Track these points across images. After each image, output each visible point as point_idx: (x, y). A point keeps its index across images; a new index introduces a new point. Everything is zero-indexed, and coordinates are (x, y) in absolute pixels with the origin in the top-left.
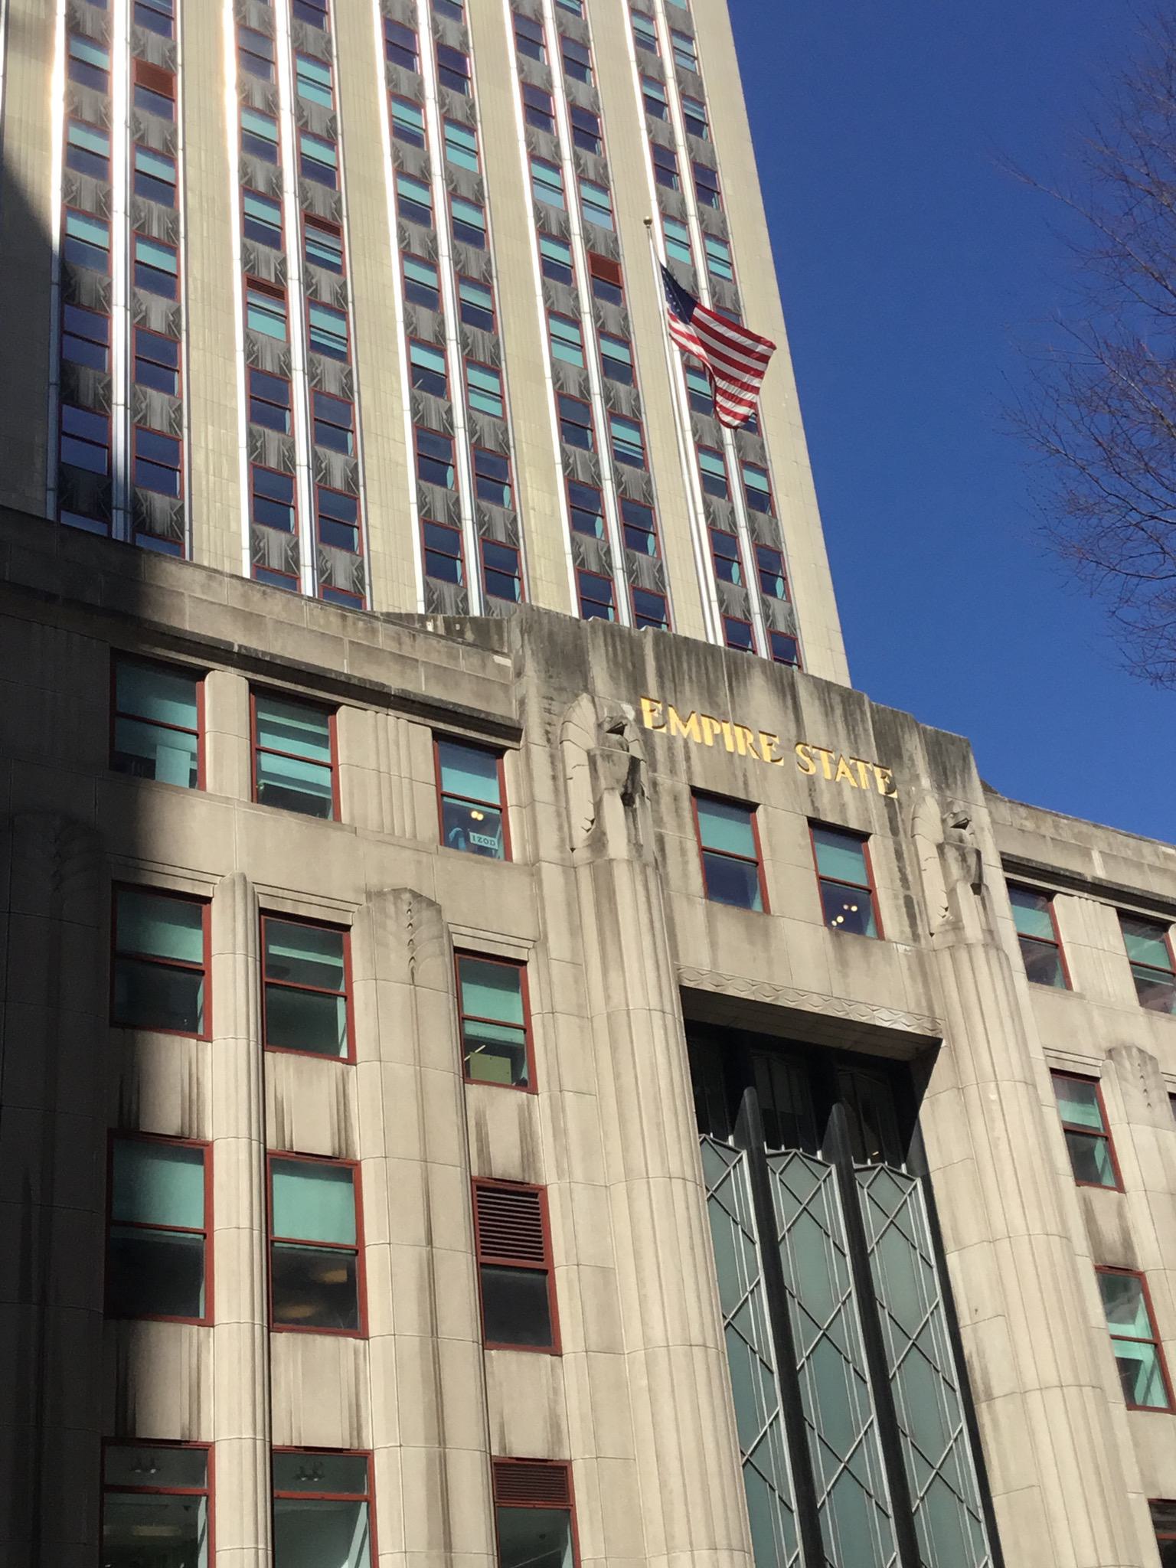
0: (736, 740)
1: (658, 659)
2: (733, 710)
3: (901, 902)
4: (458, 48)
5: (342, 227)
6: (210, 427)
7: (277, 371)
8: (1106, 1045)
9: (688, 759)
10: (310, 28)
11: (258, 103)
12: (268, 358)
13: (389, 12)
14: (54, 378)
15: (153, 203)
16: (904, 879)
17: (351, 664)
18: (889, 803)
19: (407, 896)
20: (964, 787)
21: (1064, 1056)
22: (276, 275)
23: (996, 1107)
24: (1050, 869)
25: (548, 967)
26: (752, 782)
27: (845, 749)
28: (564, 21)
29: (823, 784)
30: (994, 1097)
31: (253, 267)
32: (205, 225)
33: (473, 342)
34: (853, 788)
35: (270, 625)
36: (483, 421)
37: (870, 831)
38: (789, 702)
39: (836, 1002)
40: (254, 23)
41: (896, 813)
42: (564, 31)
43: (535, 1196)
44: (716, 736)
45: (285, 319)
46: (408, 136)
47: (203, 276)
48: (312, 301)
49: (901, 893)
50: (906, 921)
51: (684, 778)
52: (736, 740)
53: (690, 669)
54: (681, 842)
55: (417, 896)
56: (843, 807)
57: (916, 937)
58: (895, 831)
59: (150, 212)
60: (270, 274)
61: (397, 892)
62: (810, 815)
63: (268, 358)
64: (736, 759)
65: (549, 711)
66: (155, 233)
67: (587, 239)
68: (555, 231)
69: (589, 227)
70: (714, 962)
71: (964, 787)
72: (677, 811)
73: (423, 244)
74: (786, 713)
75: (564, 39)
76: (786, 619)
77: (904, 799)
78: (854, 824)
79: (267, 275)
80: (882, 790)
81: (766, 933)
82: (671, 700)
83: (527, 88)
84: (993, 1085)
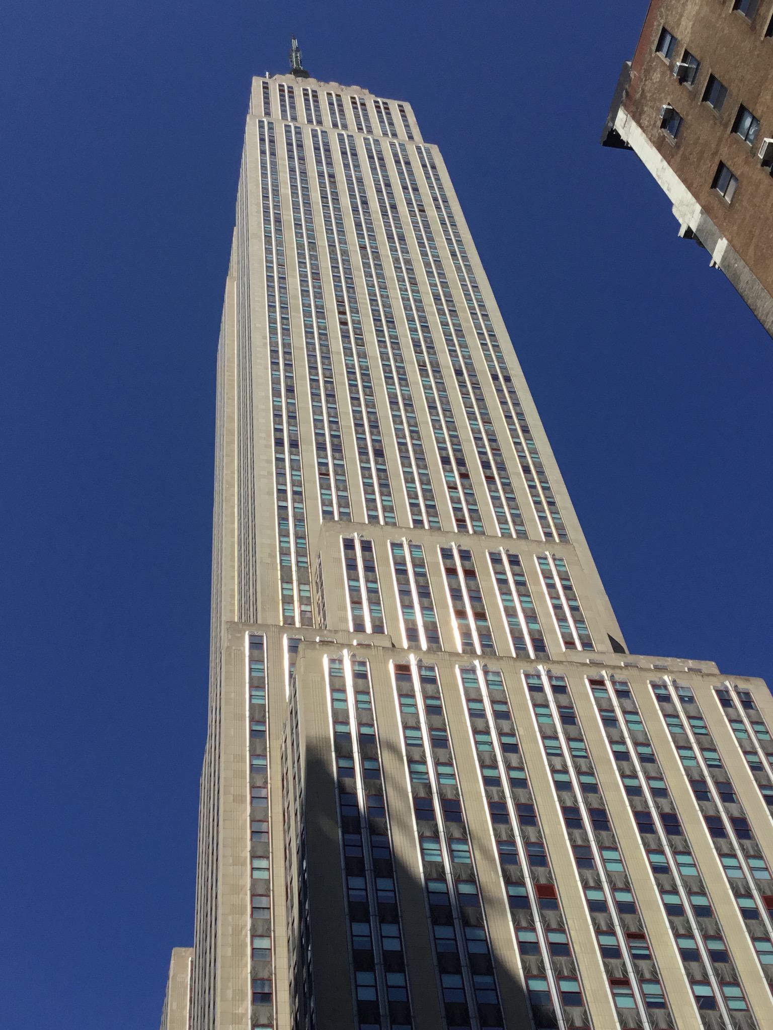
4: (670, 812)
5: (645, 933)
7: (636, 1026)
10: (604, 833)
11: (592, 884)
12: (631, 1021)
13: (635, 808)
14: (531, 1015)
15: (561, 958)
22: (623, 974)
28: (714, 774)
31: (611, 973)
32: (585, 959)
33: (722, 973)
36: (738, 1015)
40: (579, 842)
42: (716, 779)
45: (632, 995)
46: (660, 870)
47: (591, 988)
48: (642, 980)
59: (561, 964)
60: (620, 975)
63: (631, 1021)
66: (566, 974)
67: (759, 889)
68: (743, 892)
69: (759, 883)
73: (684, 927)
75: (717, 784)
79: (619, 975)
83: (708, 819)
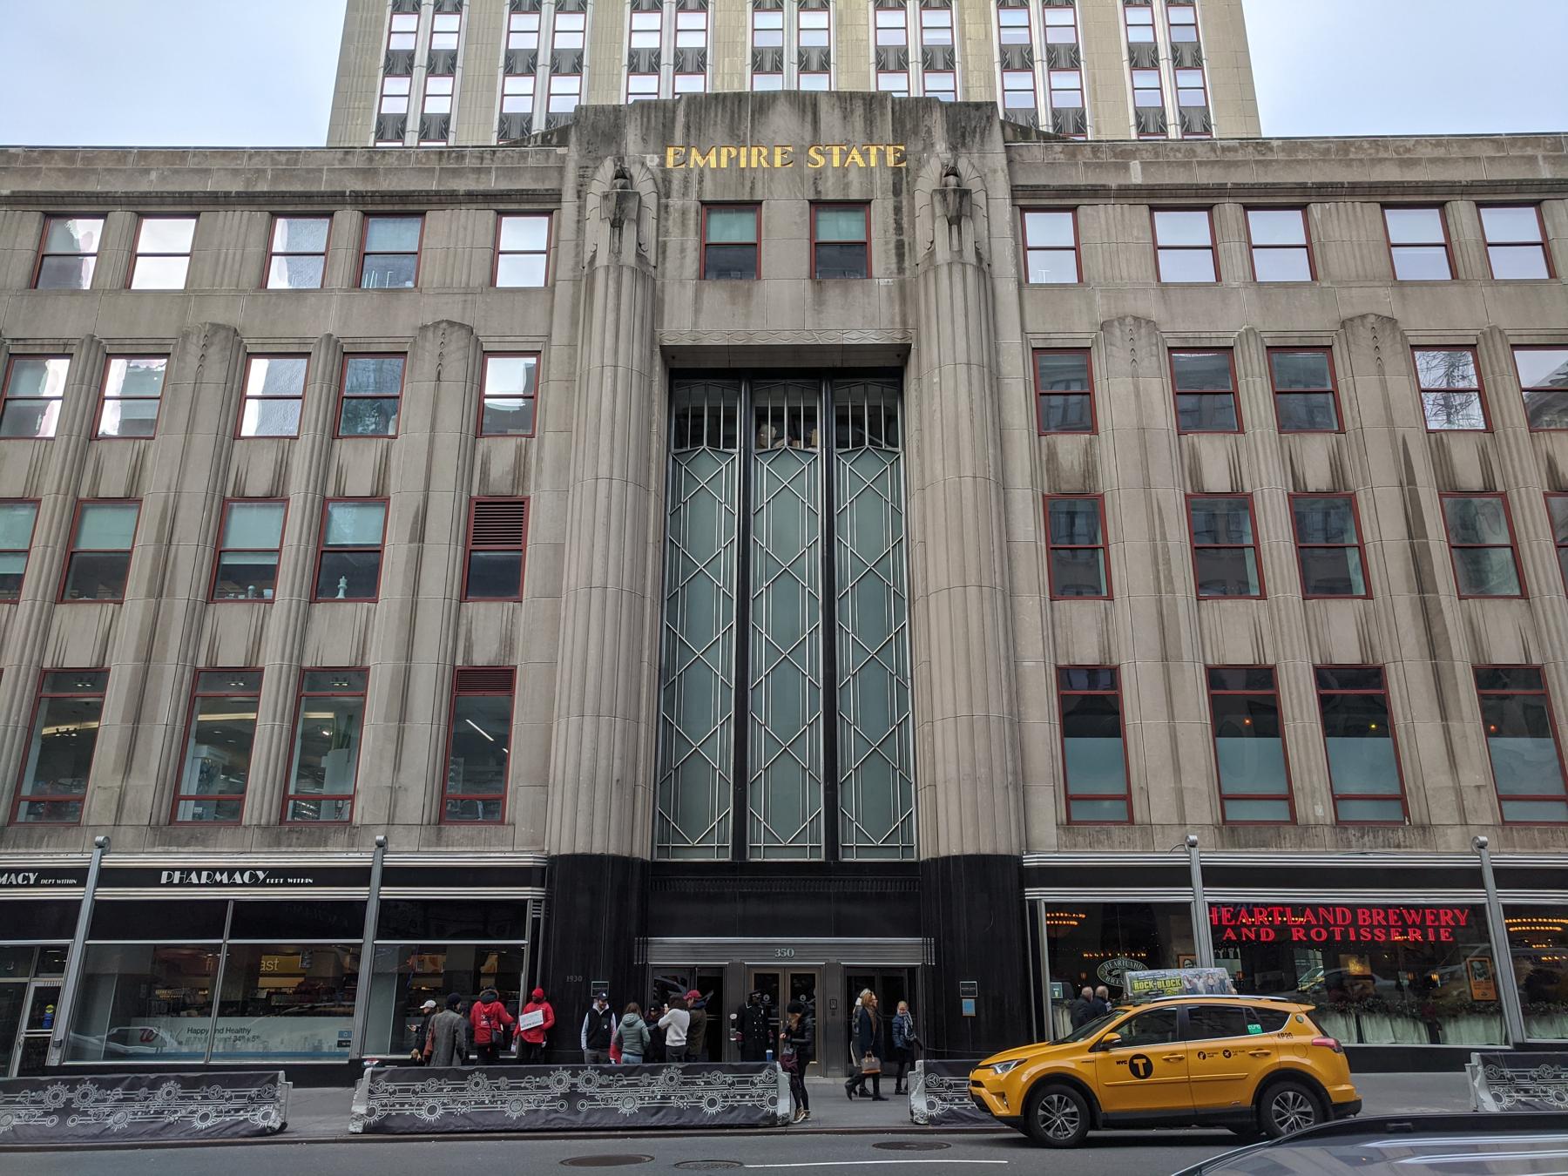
0: (752, 158)
1: (687, 115)
2: (751, 136)
3: (892, 245)
6: (727, 59)
8: (1101, 320)
9: (701, 181)
16: (899, 229)
17: (439, 183)
18: (897, 172)
19: (444, 325)
20: (982, 141)
21: (1052, 336)
23: (937, 388)
24: (1069, 188)
25: (550, 349)
26: (759, 185)
27: (859, 136)
29: (829, 173)
30: (936, 380)
34: (860, 168)
35: (382, 172)
37: (870, 198)
38: (809, 118)
39: (806, 333)
41: (902, 179)
43: (523, 503)
44: (729, 158)
49: (893, 239)
50: (893, 259)
51: (694, 196)
52: (752, 158)
53: (716, 116)
54: (682, 244)
55: (451, 323)
56: (847, 186)
57: (901, 270)
58: (897, 192)
61: (437, 324)
62: (812, 198)
64: (747, 173)
65: (583, 176)
70: (695, 324)
71: (982, 141)
72: (684, 224)
74: (803, 126)
76: (1192, 54)
77: (913, 165)
78: (855, 195)
80: (891, 161)
81: (749, 295)
82: (692, 142)
84: (937, 371)
